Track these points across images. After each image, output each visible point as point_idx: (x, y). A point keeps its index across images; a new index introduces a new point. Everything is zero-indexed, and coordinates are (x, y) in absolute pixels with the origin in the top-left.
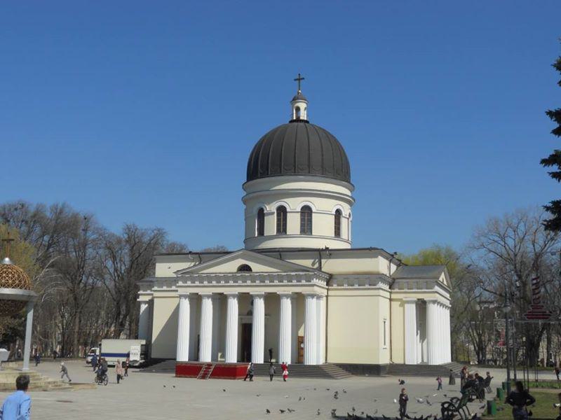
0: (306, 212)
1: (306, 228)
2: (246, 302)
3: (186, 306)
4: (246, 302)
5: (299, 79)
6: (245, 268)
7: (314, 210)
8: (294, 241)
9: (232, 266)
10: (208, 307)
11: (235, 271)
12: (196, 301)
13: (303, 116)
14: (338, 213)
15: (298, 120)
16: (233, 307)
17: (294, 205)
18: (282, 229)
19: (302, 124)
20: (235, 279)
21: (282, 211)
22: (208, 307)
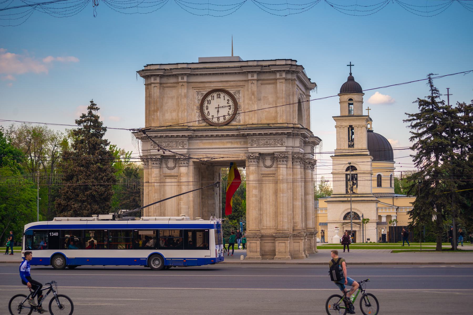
14: (391, 176)
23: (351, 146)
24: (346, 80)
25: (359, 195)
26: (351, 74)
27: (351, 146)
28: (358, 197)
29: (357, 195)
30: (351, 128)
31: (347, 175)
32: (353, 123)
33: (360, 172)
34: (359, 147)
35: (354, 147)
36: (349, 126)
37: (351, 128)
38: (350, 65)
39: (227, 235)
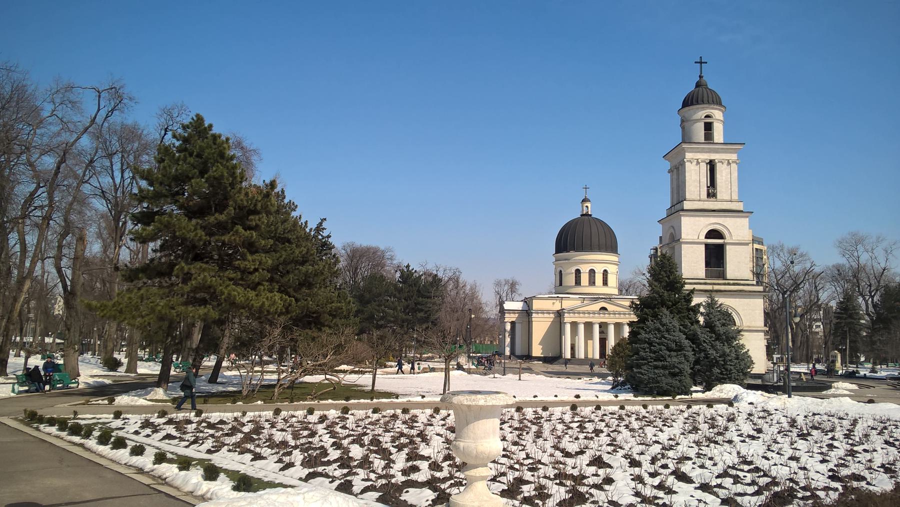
0: (605, 273)
1: (605, 283)
2: (603, 326)
3: (568, 328)
4: (603, 326)
5: (586, 188)
6: (604, 309)
7: (609, 272)
8: (599, 289)
9: (596, 307)
10: (581, 328)
11: (598, 310)
12: (574, 325)
13: (590, 213)
15: (587, 215)
16: (596, 328)
17: (599, 269)
18: (592, 282)
19: (586, 217)
20: (600, 314)
21: (592, 272)
22: (581, 328)
23: (712, 195)
24: (692, 87)
25: (731, 282)
26: (701, 77)
27: (712, 195)
28: (729, 284)
29: (727, 282)
30: (712, 165)
31: (707, 246)
32: (713, 156)
33: (735, 239)
34: (725, 198)
35: (716, 198)
36: (708, 161)
37: (712, 165)
38: (701, 63)
39: (674, 351)
